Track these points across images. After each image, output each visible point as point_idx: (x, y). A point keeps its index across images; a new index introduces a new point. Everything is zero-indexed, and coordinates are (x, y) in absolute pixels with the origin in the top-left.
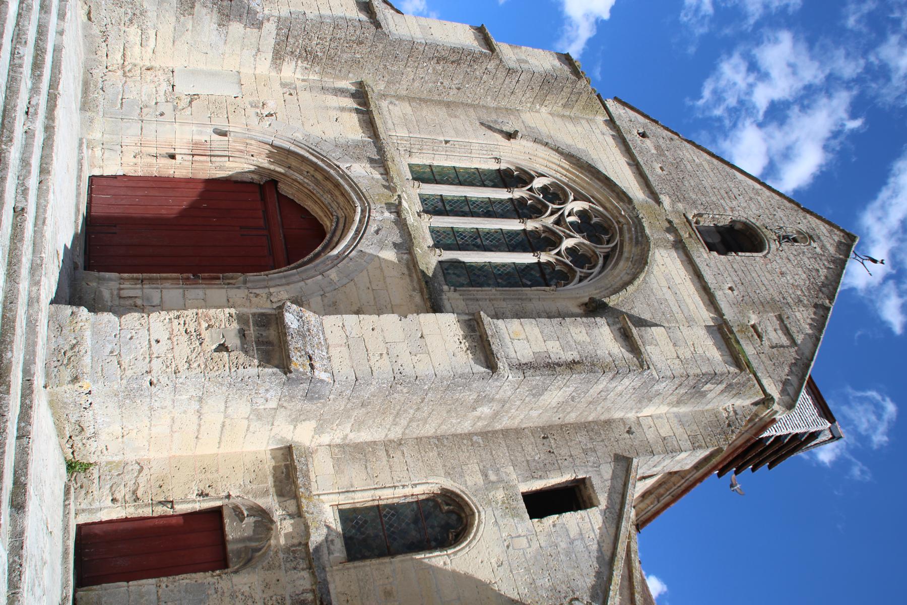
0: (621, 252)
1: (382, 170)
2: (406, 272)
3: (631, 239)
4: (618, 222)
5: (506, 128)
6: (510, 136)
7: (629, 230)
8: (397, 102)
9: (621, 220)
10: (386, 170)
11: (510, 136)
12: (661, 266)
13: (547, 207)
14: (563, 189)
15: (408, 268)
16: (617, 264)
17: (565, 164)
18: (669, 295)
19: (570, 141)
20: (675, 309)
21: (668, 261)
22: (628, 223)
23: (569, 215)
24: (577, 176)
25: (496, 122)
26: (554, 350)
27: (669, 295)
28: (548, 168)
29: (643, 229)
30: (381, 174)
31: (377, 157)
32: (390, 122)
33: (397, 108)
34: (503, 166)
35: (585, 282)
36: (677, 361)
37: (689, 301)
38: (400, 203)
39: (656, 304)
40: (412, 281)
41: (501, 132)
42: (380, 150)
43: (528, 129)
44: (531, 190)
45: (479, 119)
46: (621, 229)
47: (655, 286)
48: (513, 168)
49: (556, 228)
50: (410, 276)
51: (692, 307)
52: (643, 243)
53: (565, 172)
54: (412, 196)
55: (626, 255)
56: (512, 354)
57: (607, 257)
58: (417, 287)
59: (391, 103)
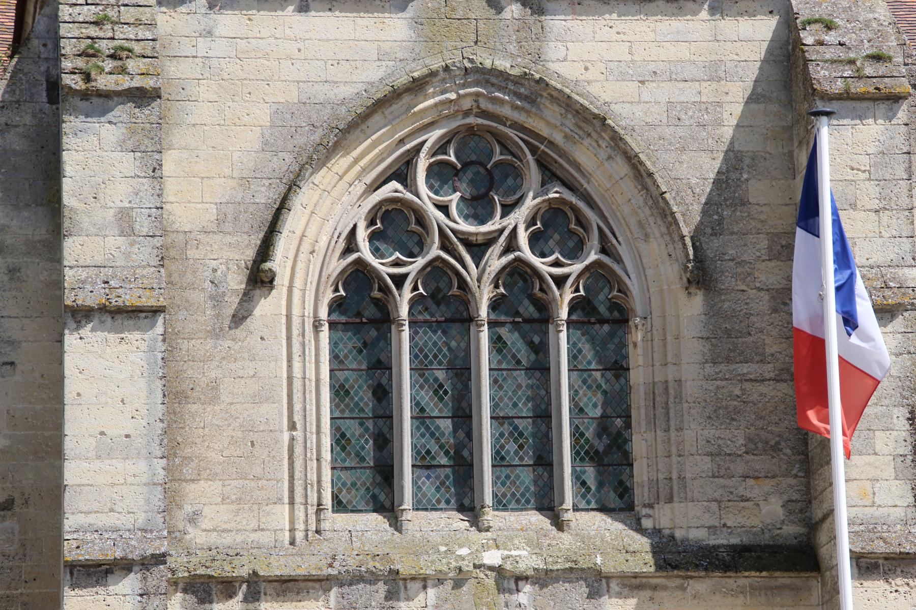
0: (551, 144)
1: (414, 586)
2: (647, 593)
3: (515, 108)
4: (467, 113)
5: (236, 282)
6: (259, 279)
7: (495, 100)
8: (188, 509)
9: (467, 104)
10: (413, 579)
11: (259, 279)
12: (589, 76)
13: (438, 258)
14: (381, 203)
15: (640, 587)
16: (578, 167)
17: (324, 177)
18: (661, 92)
19: (250, 139)
20: (688, 93)
21: (575, 51)
22: (478, 94)
23: (444, 208)
24: (356, 161)
25: (217, 300)
26: (892, 444)
27: (661, 92)
28: (331, 211)
29: (502, 74)
30: (425, 587)
31: (382, 588)
32: (254, 536)
33: (207, 511)
34: (323, 313)
35: (623, 251)
36: (885, 217)
37: (671, 52)
38: (491, 568)
39: (681, 132)
40: (665, 588)
41: (247, 298)
42: (370, 578)
43: (228, 227)
44: (399, 280)
45: (216, 334)
46: (484, 114)
47: (638, 111)
48: (329, 295)
49: (495, 261)
50: (655, 588)
51: (684, 52)
52: (533, 90)
53: (343, 184)
54: (434, 531)
55: (558, 138)
56: (899, 513)
57: (550, 174)
58: (678, 582)
59: (193, 519)
